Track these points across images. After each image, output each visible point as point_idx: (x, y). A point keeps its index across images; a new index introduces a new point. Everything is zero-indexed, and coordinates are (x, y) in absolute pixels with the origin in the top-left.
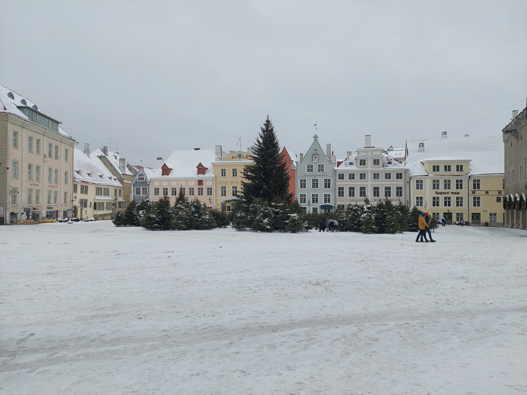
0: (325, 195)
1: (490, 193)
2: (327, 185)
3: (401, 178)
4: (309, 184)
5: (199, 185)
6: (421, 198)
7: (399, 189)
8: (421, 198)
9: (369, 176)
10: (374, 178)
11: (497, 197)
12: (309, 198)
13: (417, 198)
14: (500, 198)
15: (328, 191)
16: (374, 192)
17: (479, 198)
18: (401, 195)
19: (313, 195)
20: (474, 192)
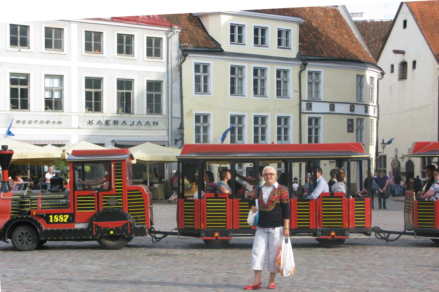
1: (339, 109)
3: (158, 54)
6: (206, 117)
7: (154, 86)
8: (206, 117)
10: (88, 48)
11: (349, 120)
13: (197, 118)
14: (352, 120)
16: (88, 95)
17: (317, 120)
18: (158, 111)
20: (309, 106)
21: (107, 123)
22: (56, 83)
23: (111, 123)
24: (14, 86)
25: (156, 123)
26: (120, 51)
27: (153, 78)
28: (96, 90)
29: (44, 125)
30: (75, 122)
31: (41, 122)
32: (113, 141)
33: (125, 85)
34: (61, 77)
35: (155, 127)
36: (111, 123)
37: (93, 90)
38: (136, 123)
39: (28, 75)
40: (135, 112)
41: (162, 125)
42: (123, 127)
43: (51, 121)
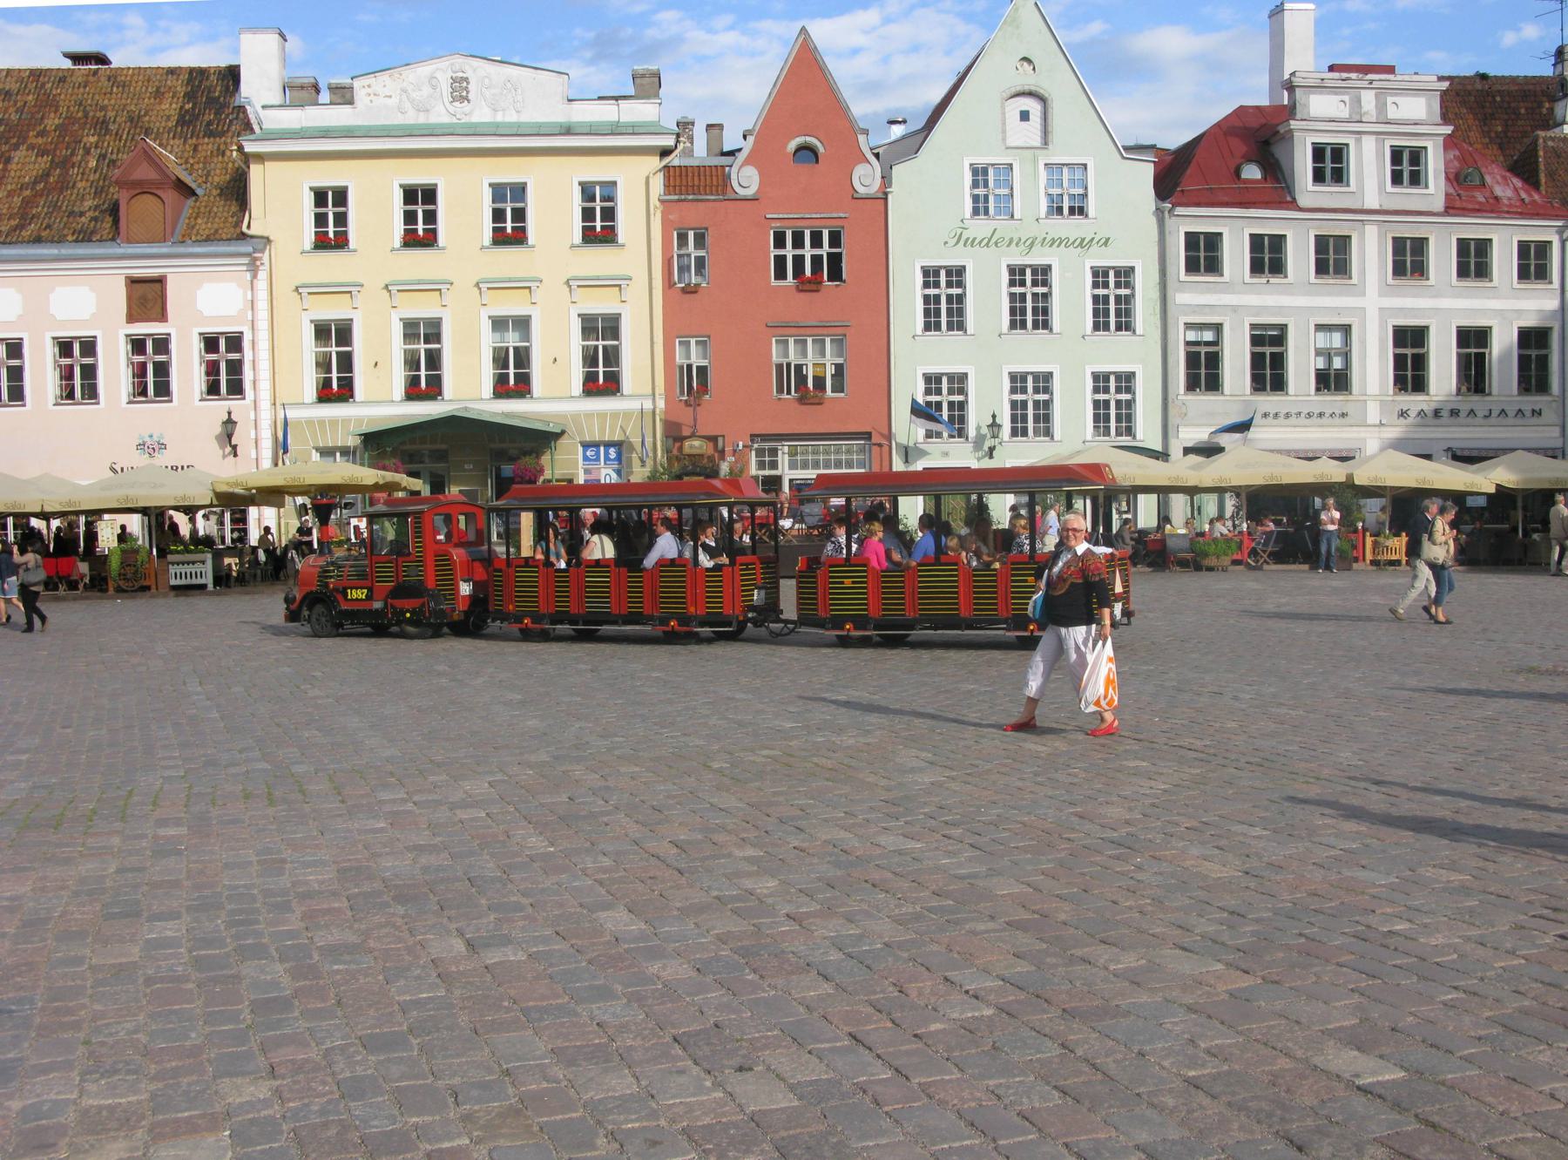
0: (1101, 380)
2: (1111, 312)
3: (1542, 274)
4: (987, 299)
5: (131, 318)
9: (1371, 252)
10: (1399, 270)
12: (988, 401)
15: (1115, 353)
16: (1399, 361)
18: (1543, 387)
19: (1018, 381)
21: (1437, 413)
22: (1336, 340)
23: (1445, 413)
24: (1259, 349)
25: (1537, 413)
26: (1463, 272)
27: (1530, 322)
28: (1416, 351)
29: (1315, 420)
30: (1373, 413)
31: (1309, 415)
32: (1449, 449)
33: (1473, 339)
34: (1346, 330)
35: (1535, 420)
36: (1445, 413)
37: (1409, 351)
38: (1495, 414)
39: (1283, 328)
40: (1495, 391)
41: (1550, 415)
42: (1470, 420)
43: (1328, 412)
